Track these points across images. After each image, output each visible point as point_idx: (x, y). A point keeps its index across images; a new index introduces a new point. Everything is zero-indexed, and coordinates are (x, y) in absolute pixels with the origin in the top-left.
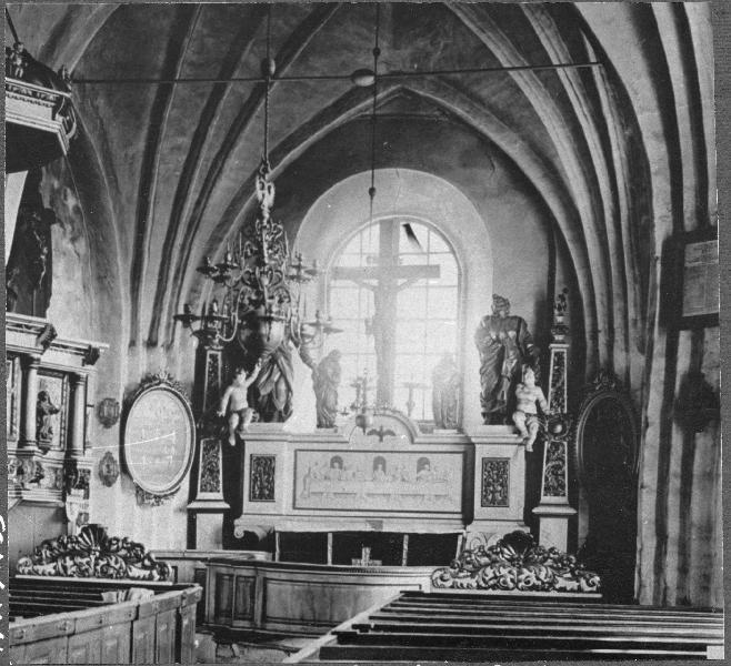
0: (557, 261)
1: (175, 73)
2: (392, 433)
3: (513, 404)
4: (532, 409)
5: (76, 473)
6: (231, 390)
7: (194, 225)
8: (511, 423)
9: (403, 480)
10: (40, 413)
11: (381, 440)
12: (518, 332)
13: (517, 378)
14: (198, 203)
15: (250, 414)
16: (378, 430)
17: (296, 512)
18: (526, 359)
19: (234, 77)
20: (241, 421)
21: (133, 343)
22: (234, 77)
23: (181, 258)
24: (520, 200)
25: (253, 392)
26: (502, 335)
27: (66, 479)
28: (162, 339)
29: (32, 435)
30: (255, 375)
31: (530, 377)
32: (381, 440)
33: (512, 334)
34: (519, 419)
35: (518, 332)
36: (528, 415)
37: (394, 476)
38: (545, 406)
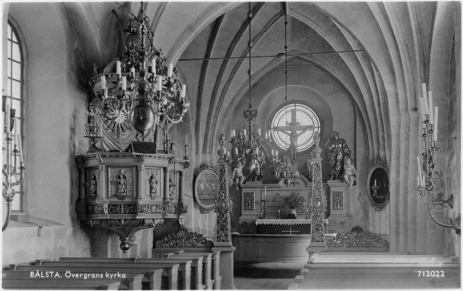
1: (209, 55)
3: (342, 171)
5: (183, 207)
6: (236, 169)
7: (218, 109)
8: (342, 180)
10: (170, 186)
12: (343, 144)
13: (343, 163)
14: (220, 100)
19: (231, 57)
20: (240, 180)
21: (197, 153)
22: (231, 57)
23: (214, 121)
24: (342, 95)
27: (179, 210)
28: (208, 151)
29: (168, 196)
31: (349, 162)
33: (340, 145)
34: (346, 177)
35: (343, 144)
36: (349, 176)
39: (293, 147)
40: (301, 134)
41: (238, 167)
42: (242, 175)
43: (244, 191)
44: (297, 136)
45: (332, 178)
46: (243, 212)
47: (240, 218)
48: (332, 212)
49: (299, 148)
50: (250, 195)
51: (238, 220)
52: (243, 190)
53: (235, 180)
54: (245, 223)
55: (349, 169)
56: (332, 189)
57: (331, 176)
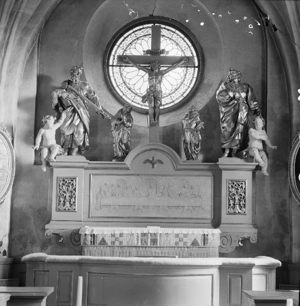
0: (268, 49)
2: (161, 162)
3: (245, 142)
4: (260, 146)
6: (42, 131)
9: (169, 196)
11: (153, 167)
12: (247, 93)
15: (57, 149)
16: (151, 159)
17: (90, 220)
18: (252, 113)
20: (50, 151)
25: (59, 133)
26: (237, 95)
30: (62, 121)
31: (260, 122)
32: (153, 167)
33: (243, 95)
35: (247, 93)
37: (162, 193)
38: (268, 143)
39: (153, 96)
40: (166, 71)
41: (48, 128)
42: (54, 142)
43: (58, 173)
44: (162, 74)
45: (226, 155)
46: (55, 215)
47: (47, 226)
48: (224, 217)
49: (164, 101)
50: (69, 183)
51: (44, 230)
52: (55, 170)
53: (40, 150)
54: (57, 236)
55: (258, 135)
56: (226, 176)
57: (224, 150)
